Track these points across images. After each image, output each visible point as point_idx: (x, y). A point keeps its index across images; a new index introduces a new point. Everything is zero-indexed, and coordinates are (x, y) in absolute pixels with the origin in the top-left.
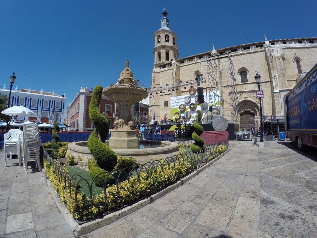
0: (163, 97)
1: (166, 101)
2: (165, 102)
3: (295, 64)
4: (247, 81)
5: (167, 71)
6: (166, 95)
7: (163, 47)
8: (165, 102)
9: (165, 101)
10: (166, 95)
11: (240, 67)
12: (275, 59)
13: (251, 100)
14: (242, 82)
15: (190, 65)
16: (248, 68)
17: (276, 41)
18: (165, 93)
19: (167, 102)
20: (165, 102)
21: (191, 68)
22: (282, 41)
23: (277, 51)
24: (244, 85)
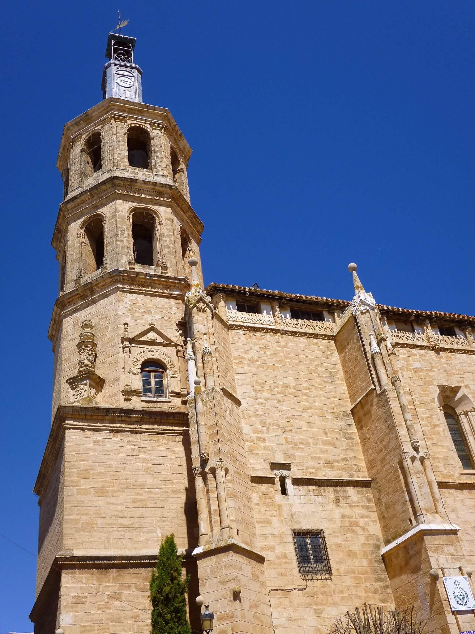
0: (279, 497)
1: (306, 525)
5: (278, 336)
6: (297, 482)
9: (297, 527)
10: (297, 482)
15: (410, 351)
18: (286, 466)
20: (299, 535)
21: (417, 365)
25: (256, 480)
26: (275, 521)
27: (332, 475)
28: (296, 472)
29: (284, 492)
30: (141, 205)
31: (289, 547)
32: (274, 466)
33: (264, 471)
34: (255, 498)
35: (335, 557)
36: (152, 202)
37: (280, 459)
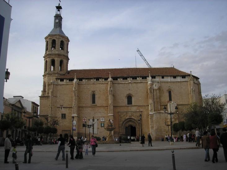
0: (61, 110)
1: (64, 113)
2: (62, 114)
3: (168, 94)
4: (131, 104)
7: (59, 55)
8: (62, 114)
10: (63, 108)
11: (128, 93)
12: (153, 90)
13: (134, 118)
14: (128, 104)
16: (133, 95)
17: (157, 76)
18: (63, 105)
19: (65, 114)
20: (62, 114)
21: (88, 88)
22: (162, 76)
23: (156, 85)
24: (129, 107)
25: (58, 108)
26: (60, 113)
27: (69, 106)
28: (64, 106)
29: (62, 109)
30: (52, 58)
31: (61, 116)
32: (60, 106)
33: (59, 106)
34: (57, 110)
35: (66, 117)
36: (54, 57)
37: (62, 104)
